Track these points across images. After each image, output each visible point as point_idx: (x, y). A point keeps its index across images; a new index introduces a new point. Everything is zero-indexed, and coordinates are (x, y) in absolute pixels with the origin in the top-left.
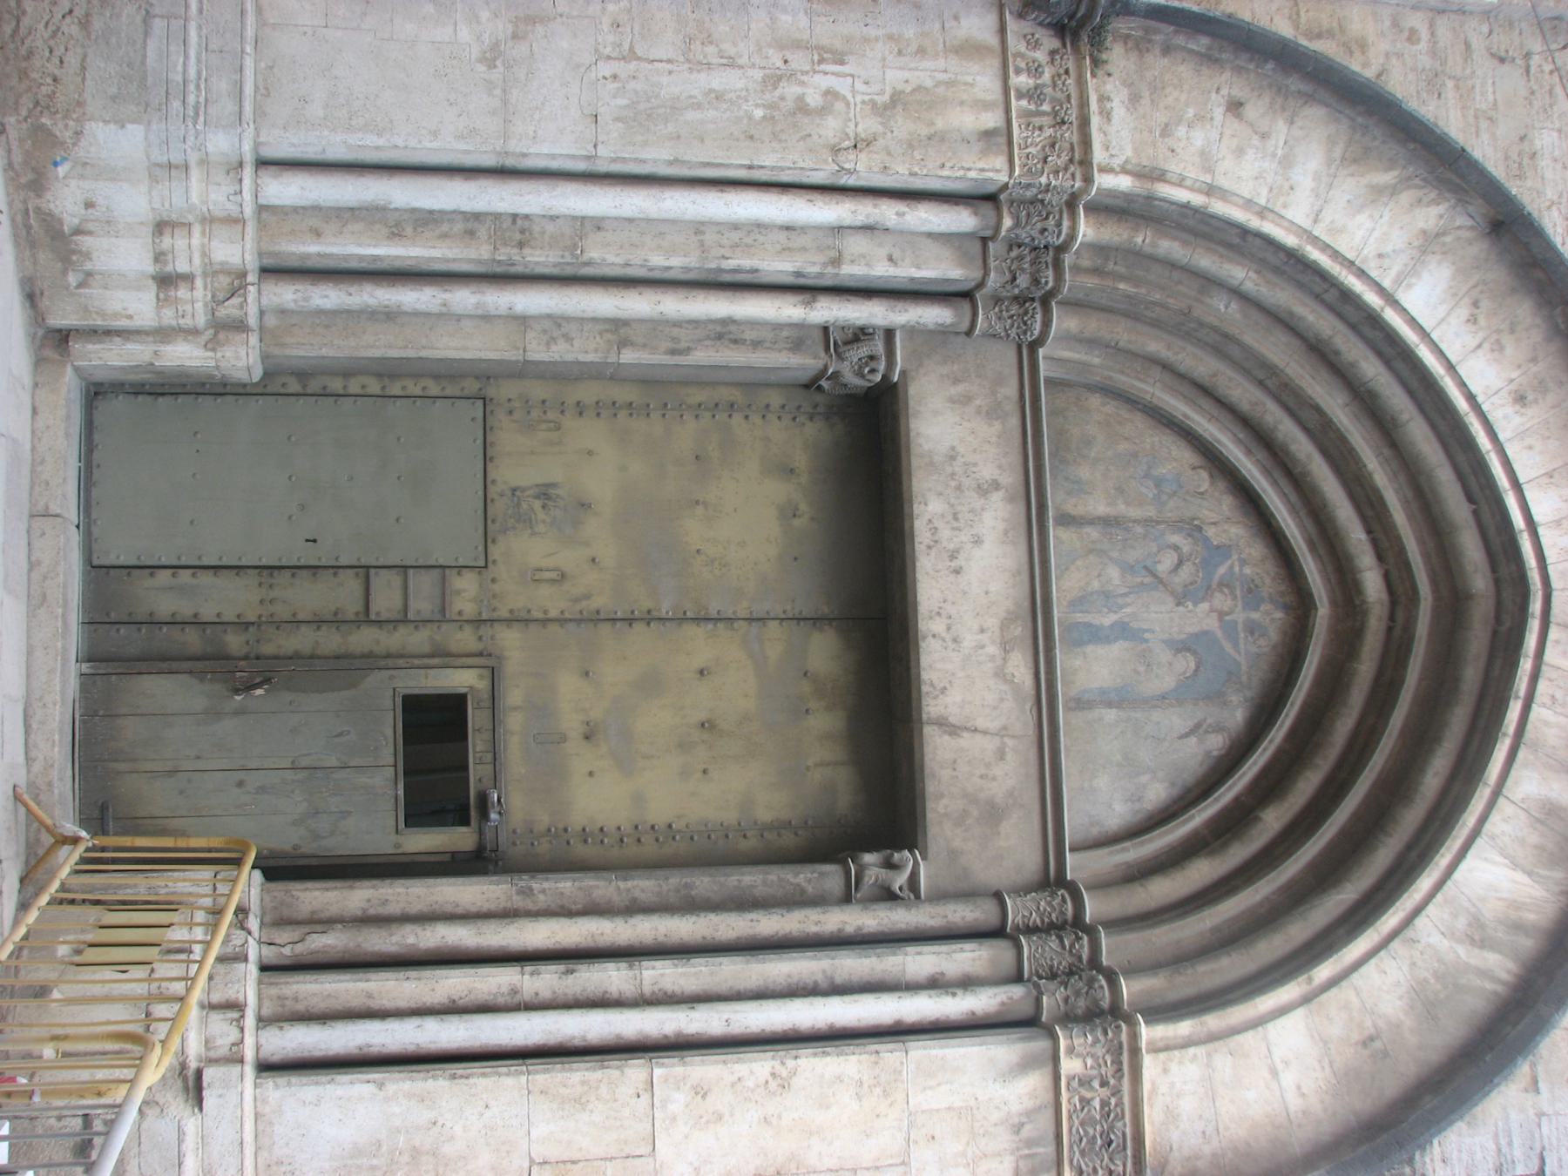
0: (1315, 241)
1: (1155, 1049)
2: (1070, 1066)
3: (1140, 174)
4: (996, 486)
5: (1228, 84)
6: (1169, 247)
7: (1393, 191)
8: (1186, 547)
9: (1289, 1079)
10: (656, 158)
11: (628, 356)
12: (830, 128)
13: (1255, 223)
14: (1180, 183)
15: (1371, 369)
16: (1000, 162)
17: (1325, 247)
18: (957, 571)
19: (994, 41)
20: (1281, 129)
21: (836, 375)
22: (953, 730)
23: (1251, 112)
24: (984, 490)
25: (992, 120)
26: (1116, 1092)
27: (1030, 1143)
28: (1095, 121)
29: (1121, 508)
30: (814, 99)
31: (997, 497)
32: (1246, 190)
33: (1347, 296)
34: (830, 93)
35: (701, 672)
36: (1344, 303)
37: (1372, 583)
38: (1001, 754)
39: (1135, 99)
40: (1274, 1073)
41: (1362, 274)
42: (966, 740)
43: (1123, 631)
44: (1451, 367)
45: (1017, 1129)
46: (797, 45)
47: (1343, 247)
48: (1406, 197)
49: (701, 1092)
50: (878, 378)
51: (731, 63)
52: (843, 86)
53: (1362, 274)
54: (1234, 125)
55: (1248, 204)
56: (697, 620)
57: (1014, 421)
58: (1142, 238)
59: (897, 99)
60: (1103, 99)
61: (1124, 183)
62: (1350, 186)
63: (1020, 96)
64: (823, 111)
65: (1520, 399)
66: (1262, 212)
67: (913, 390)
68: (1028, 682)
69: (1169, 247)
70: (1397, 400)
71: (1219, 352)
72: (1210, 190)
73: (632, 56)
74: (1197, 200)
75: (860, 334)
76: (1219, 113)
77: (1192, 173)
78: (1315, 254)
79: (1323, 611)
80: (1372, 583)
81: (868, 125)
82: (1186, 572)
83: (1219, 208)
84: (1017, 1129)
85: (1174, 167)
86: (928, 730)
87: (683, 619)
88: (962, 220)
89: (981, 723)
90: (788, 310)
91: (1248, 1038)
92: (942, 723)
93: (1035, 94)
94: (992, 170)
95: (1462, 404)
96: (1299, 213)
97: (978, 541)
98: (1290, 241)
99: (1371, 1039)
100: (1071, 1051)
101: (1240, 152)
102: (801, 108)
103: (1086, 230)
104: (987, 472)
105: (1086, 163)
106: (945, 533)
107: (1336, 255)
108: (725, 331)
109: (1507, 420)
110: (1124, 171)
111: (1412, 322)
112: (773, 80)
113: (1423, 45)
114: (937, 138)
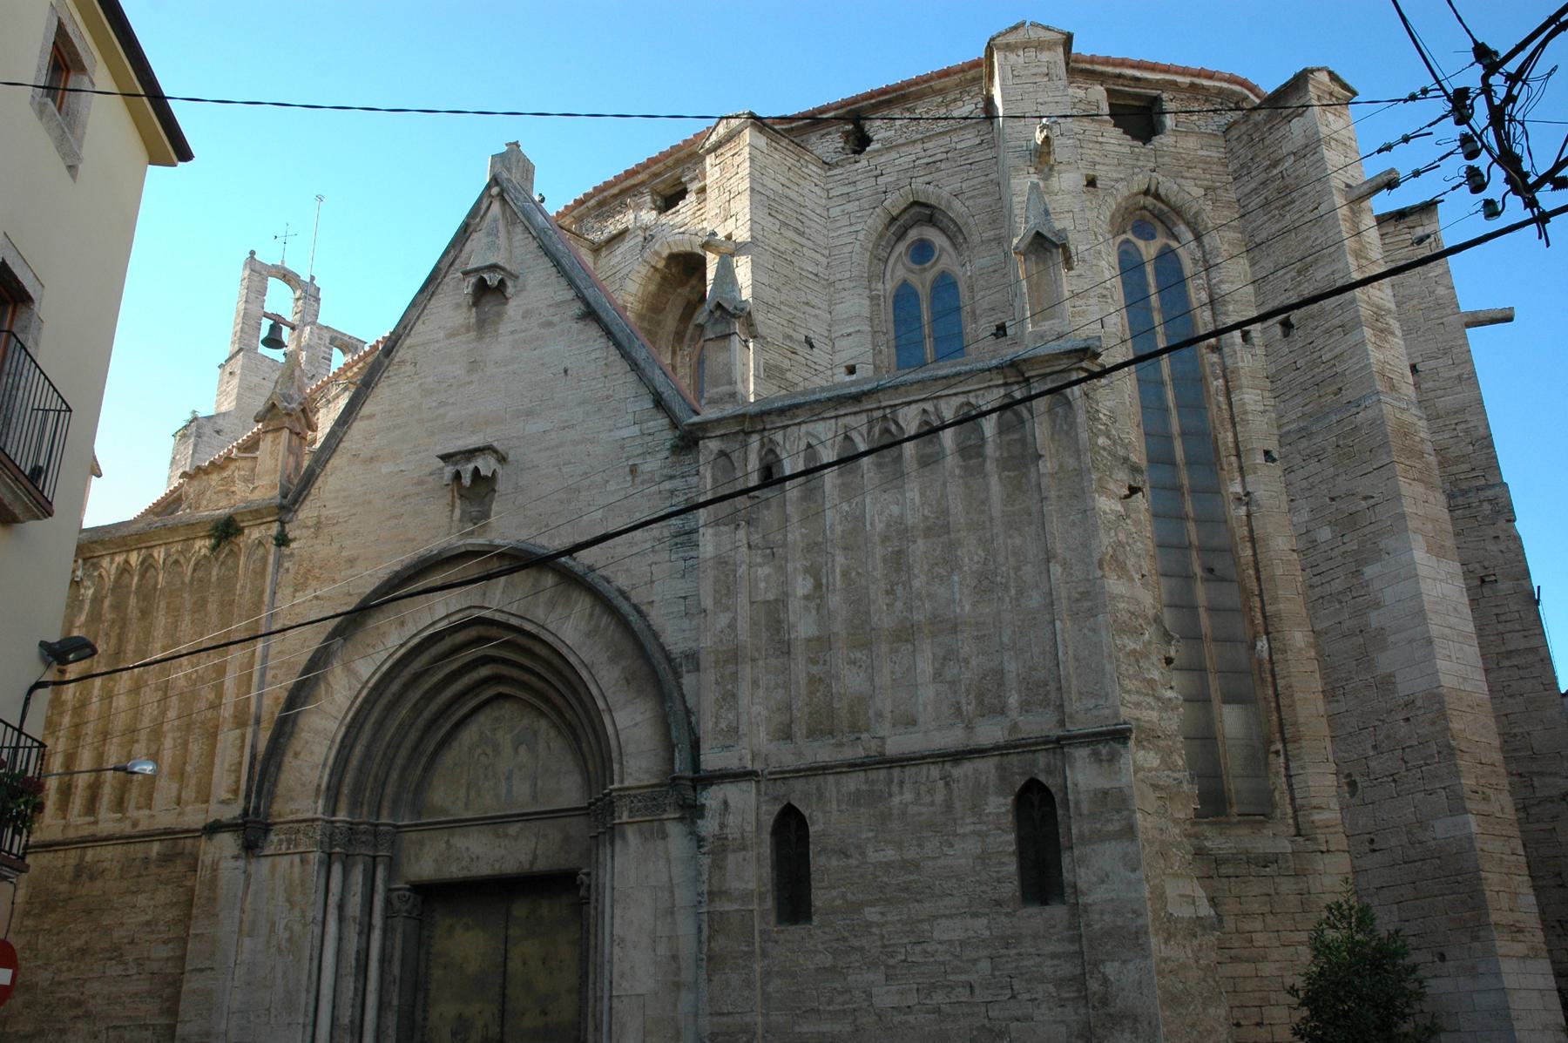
0: (344, 718)
1: (622, 781)
2: (625, 818)
3: (317, 795)
4: (447, 842)
5: (288, 759)
6: (349, 778)
7: (328, 684)
8: (479, 751)
9: (639, 718)
10: (304, 999)
11: (395, 1002)
12: (297, 927)
13: (336, 745)
14: (321, 777)
15: (395, 687)
16: (311, 856)
17: (347, 713)
18: (478, 858)
19: (271, 859)
20: (305, 735)
21: (407, 911)
22: (535, 857)
23: (298, 749)
24: (449, 845)
25: (297, 859)
26: (635, 796)
27: (652, 834)
28: (300, 816)
29: (463, 781)
30: (287, 934)
31: (452, 841)
32: (325, 749)
33: (366, 701)
34: (285, 929)
35: (524, 964)
36: (369, 703)
37: (484, 671)
38: (545, 836)
39: (292, 799)
40: (636, 725)
41: (356, 697)
42: (539, 852)
43: (509, 778)
44: (391, 655)
45: (646, 839)
46: (268, 942)
47: (346, 707)
48: (330, 678)
49: (622, 976)
50: (407, 893)
51: (273, 968)
52: (284, 922)
53: (356, 697)
54: (302, 756)
55: (330, 748)
56: (505, 966)
57: (426, 833)
58: (345, 790)
59: (288, 900)
60: (292, 813)
61: (321, 803)
62: (324, 702)
63: (289, 848)
64: (291, 931)
65: (402, 624)
66: (333, 741)
67: (412, 879)
68: (520, 825)
69: (349, 778)
70: (407, 674)
71: (399, 746)
72: (325, 765)
73: (269, 1010)
74: (327, 771)
75: (388, 902)
76: (299, 762)
77: (318, 774)
78: (348, 718)
79: (502, 689)
80: (484, 671)
81: (297, 912)
82: (489, 751)
83: (330, 762)
84: (646, 839)
85: (316, 782)
86: (535, 869)
87: (505, 973)
88: (337, 869)
89: (533, 846)
90: (376, 936)
91: (622, 738)
92: (532, 863)
93: (289, 841)
94: (315, 857)
95: (403, 651)
96: (332, 726)
97: (468, 849)
98: (343, 729)
99: (627, 680)
100: (620, 818)
101: (312, 753)
102: (290, 940)
103: (342, 816)
104: (443, 846)
105: (313, 820)
106: (464, 864)
107: (350, 708)
108: (384, 961)
109: (411, 629)
110: (316, 803)
111: (374, 674)
112: (280, 951)
113: (278, 672)
114: (303, 882)
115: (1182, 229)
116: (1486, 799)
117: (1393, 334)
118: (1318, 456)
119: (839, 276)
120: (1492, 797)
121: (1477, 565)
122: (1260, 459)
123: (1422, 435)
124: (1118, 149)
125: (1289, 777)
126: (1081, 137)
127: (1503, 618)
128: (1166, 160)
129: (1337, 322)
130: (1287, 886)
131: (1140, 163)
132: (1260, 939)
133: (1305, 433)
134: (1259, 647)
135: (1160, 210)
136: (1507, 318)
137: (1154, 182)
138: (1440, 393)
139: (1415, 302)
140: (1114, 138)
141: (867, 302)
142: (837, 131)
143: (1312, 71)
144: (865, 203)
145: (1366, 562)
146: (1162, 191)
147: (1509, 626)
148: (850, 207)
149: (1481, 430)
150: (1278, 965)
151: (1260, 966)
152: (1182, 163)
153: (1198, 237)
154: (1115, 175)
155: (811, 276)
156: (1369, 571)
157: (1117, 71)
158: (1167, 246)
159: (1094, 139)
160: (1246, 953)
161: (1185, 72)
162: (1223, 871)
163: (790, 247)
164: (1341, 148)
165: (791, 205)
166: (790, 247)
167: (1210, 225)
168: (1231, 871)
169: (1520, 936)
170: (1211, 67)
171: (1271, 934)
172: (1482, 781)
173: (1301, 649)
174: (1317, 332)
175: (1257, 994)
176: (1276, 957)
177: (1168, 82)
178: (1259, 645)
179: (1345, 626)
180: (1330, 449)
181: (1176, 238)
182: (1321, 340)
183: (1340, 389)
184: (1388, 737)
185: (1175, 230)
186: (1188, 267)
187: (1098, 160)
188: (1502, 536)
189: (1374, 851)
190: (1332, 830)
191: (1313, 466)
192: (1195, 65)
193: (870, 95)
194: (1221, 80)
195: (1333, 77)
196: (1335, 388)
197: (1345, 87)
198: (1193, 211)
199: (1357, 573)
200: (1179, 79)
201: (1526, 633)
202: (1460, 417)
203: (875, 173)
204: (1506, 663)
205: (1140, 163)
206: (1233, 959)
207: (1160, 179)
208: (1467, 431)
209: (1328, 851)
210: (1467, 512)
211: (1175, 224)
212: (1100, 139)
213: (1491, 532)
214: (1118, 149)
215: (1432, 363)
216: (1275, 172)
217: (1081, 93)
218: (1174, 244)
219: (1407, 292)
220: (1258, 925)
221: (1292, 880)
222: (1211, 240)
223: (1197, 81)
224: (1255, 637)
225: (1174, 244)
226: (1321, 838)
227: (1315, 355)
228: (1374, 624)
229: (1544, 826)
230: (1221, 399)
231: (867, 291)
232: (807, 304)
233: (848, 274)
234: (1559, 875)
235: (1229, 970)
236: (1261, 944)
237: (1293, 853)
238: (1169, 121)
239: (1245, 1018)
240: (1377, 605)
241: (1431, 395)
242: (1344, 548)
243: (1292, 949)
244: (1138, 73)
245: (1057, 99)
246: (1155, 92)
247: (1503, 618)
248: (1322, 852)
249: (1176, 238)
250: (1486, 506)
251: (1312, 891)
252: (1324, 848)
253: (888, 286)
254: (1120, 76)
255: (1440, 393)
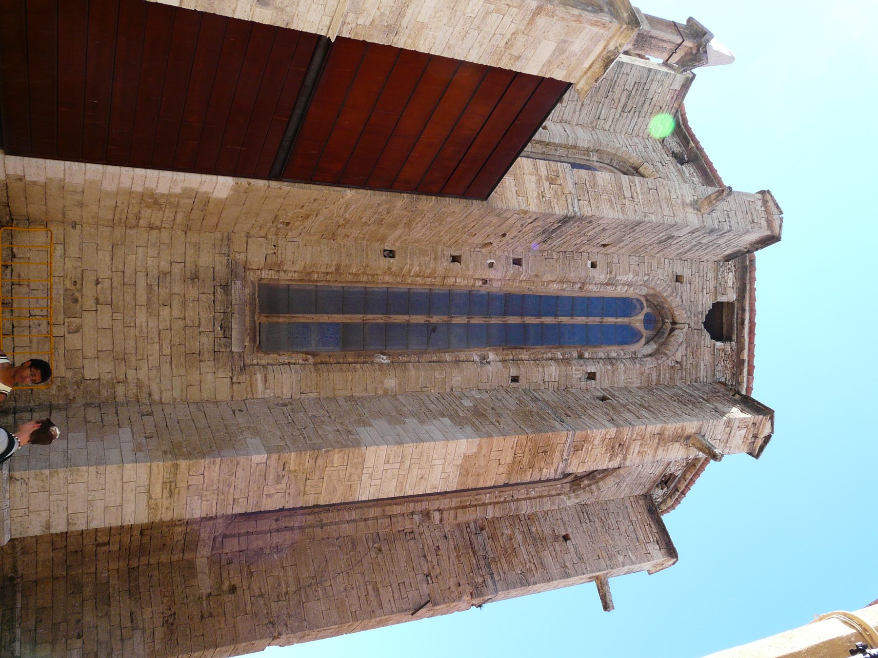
115: (653, 347)
116: (278, 479)
117: (611, 459)
118: (520, 402)
119: (599, 133)
120: (279, 486)
121: (438, 571)
122: (514, 372)
123: (545, 470)
124: (700, 303)
125: (289, 364)
126: (705, 277)
127: (402, 587)
128: (696, 337)
129: (615, 418)
130: (206, 342)
131: (693, 316)
132: (165, 312)
133: (535, 400)
134: (382, 356)
135: (664, 333)
136: (606, 606)
137: (682, 326)
138: (554, 554)
139: (610, 541)
140: (706, 303)
141: (586, 146)
142: (682, 150)
143: (772, 418)
144: (644, 154)
145: (451, 417)
146: (676, 332)
147: (396, 590)
148: (640, 147)
149: (531, 580)
150: (144, 325)
151: (144, 309)
152: (695, 349)
153: (650, 355)
154: (684, 297)
155: (598, 115)
156: (446, 420)
157: (747, 308)
158: (641, 337)
159: (705, 287)
160: (155, 299)
161: (751, 355)
162: (219, 290)
163: (616, 97)
164: (725, 437)
165: (640, 103)
166: (616, 97)
167: (660, 362)
168: (219, 297)
169: (166, 493)
170: (756, 373)
171: (168, 323)
172: (292, 478)
173: (383, 384)
174: (605, 409)
175: (121, 303)
176: (151, 324)
177: (743, 344)
178: (385, 357)
179: (403, 408)
180: (527, 408)
181: (647, 343)
182: (599, 410)
183: (570, 416)
184: (322, 421)
185: (652, 343)
186: (632, 348)
187: (693, 286)
188: (460, 589)
189: (234, 412)
190: (249, 389)
191: (513, 402)
192: (756, 362)
193: (710, 164)
194: (748, 382)
195: (768, 438)
196: (569, 413)
197: (761, 449)
198: (667, 352)
199: (443, 415)
200: (746, 352)
201: (392, 601)
202: (539, 566)
203: (663, 162)
204: (370, 588)
205: (693, 316)
206: (149, 286)
207: (685, 330)
208: (530, 570)
209: (232, 383)
210: (475, 567)
211: (655, 342)
212: (705, 291)
213: (463, 581)
214: (700, 303)
215: (572, 550)
216: (701, 400)
217: (730, 284)
218: (643, 341)
219: (616, 538)
220: (176, 313)
221: (211, 347)
222: (650, 363)
223: (746, 364)
224: (388, 355)
225: (643, 341)
226: (243, 378)
227: (588, 407)
228: (407, 420)
229: (249, 607)
230: (549, 355)
231: (592, 148)
232: (582, 105)
233: (601, 137)
234: (211, 615)
235: (142, 282)
236: (161, 313)
237: (231, 352)
238: (719, 344)
239: (103, 289)
240: (422, 422)
241: (551, 548)
242: (459, 411)
243: (156, 340)
244: (747, 322)
245: (740, 224)
246: (734, 337)
247: (402, 587)
248: (231, 378)
249: (647, 343)
250: (480, 580)
251: (202, 363)
252: (234, 380)
253: (596, 164)
254: (744, 310)
255: (554, 554)
